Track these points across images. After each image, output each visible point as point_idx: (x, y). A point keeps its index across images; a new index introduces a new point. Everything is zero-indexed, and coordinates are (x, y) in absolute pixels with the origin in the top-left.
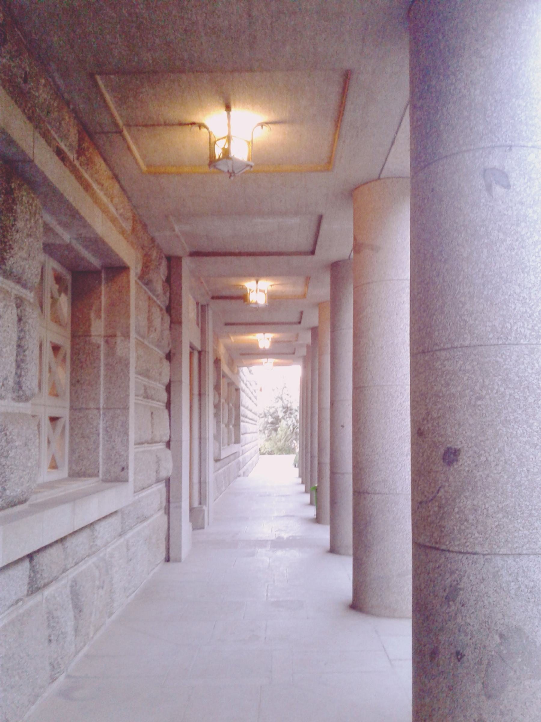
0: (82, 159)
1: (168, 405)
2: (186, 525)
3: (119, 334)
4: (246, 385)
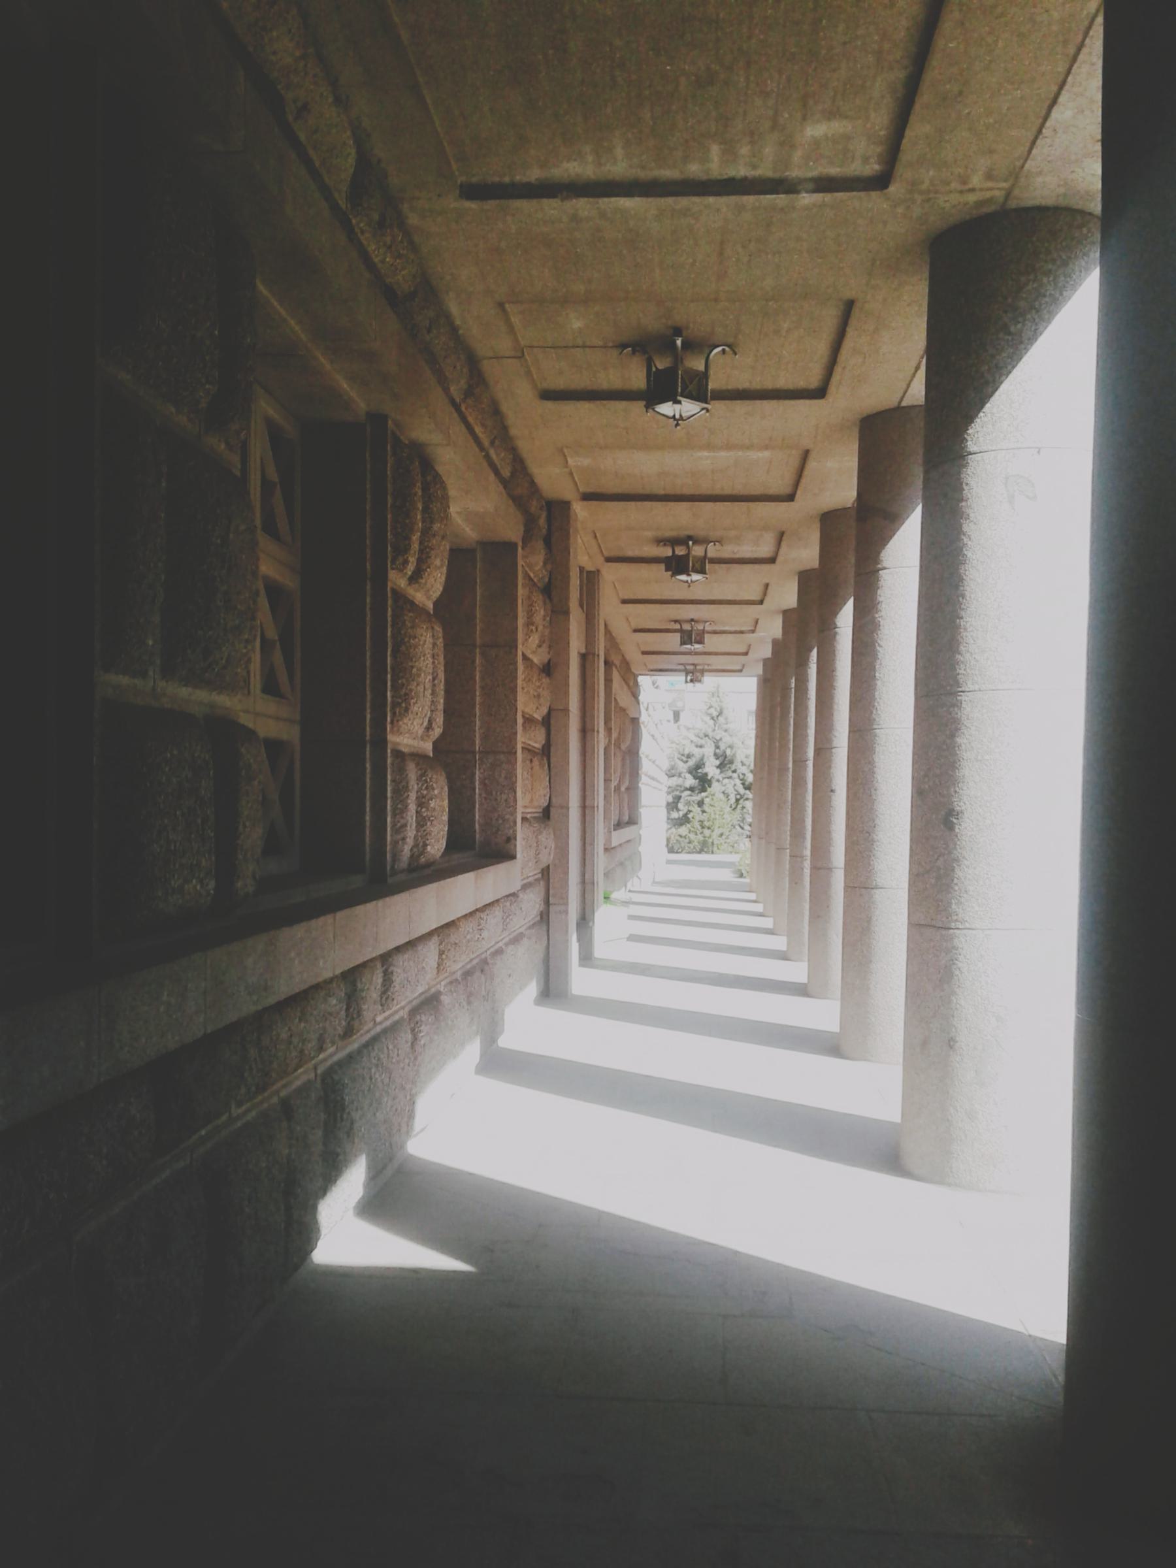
0: (470, 401)
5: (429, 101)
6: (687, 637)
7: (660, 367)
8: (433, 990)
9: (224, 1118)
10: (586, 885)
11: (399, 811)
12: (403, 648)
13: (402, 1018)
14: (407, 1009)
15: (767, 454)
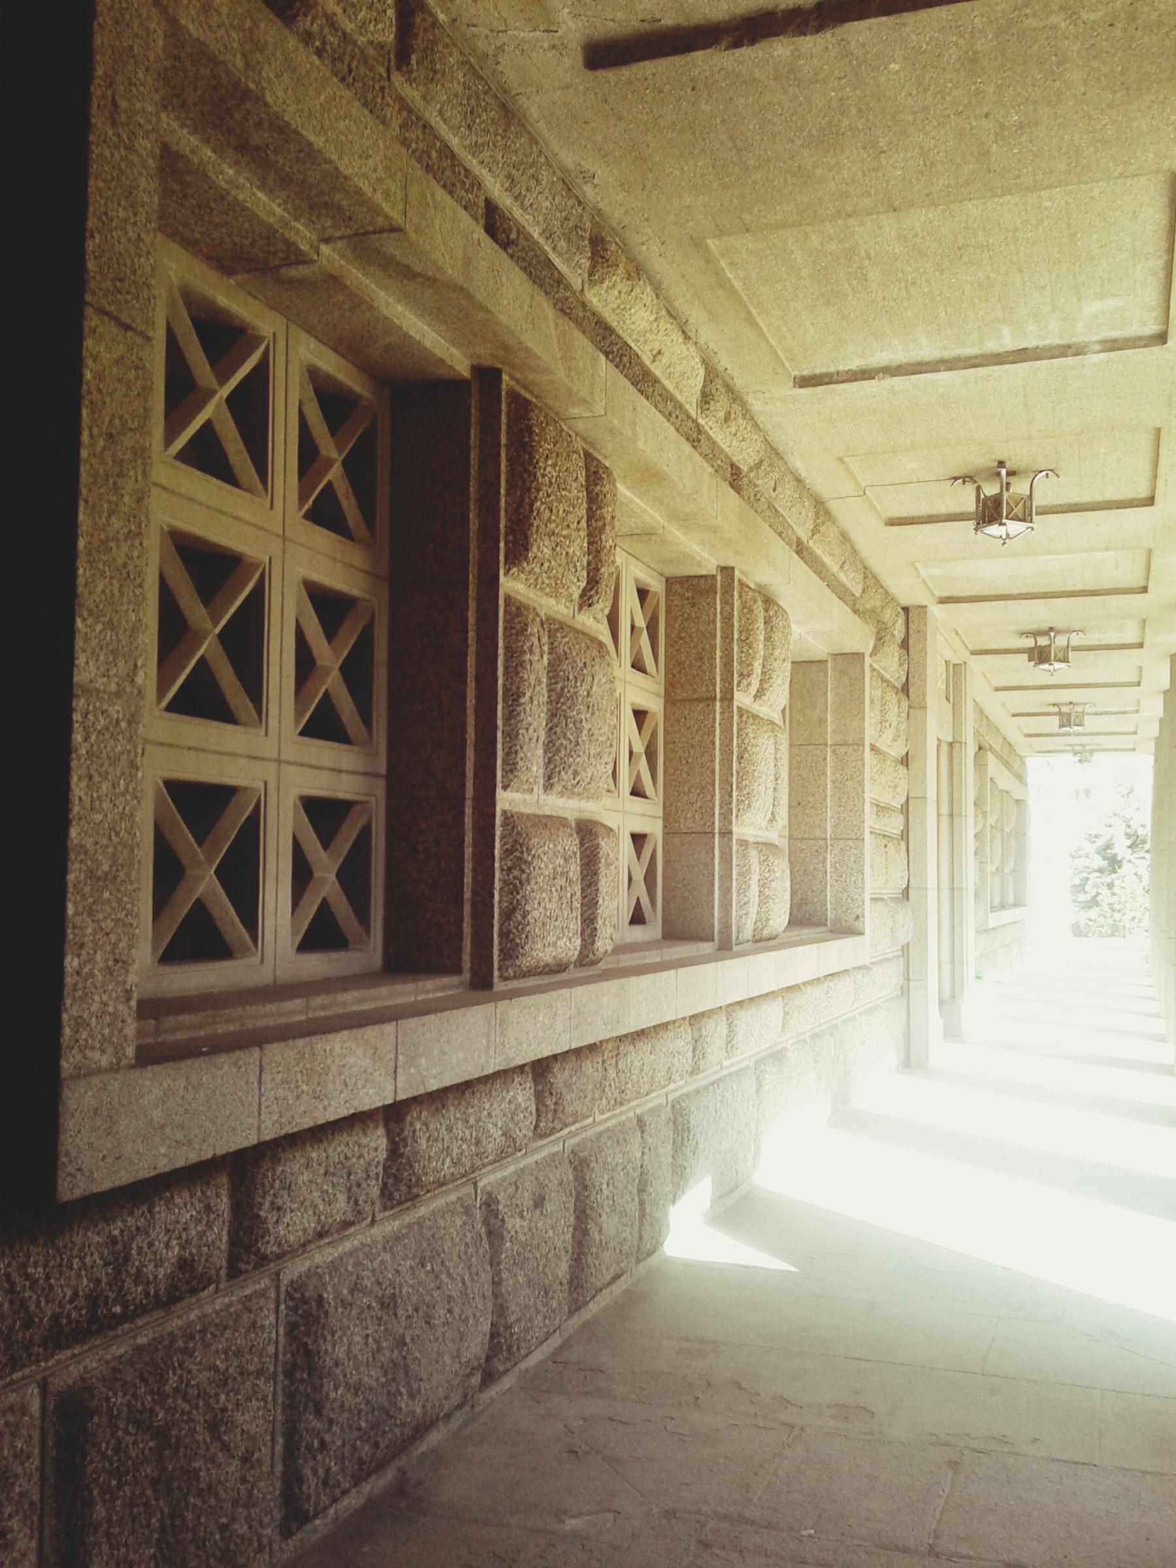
2: (935, 1022)
5: (762, 324)
6: (1066, 720)
7: (988, 494)
8: (780, 1047)
9: (590, 1120)
10: (955, 962)
11: (743, 891)
12: (746, 755)
13: (748, 1067)
14: (753, 1060)
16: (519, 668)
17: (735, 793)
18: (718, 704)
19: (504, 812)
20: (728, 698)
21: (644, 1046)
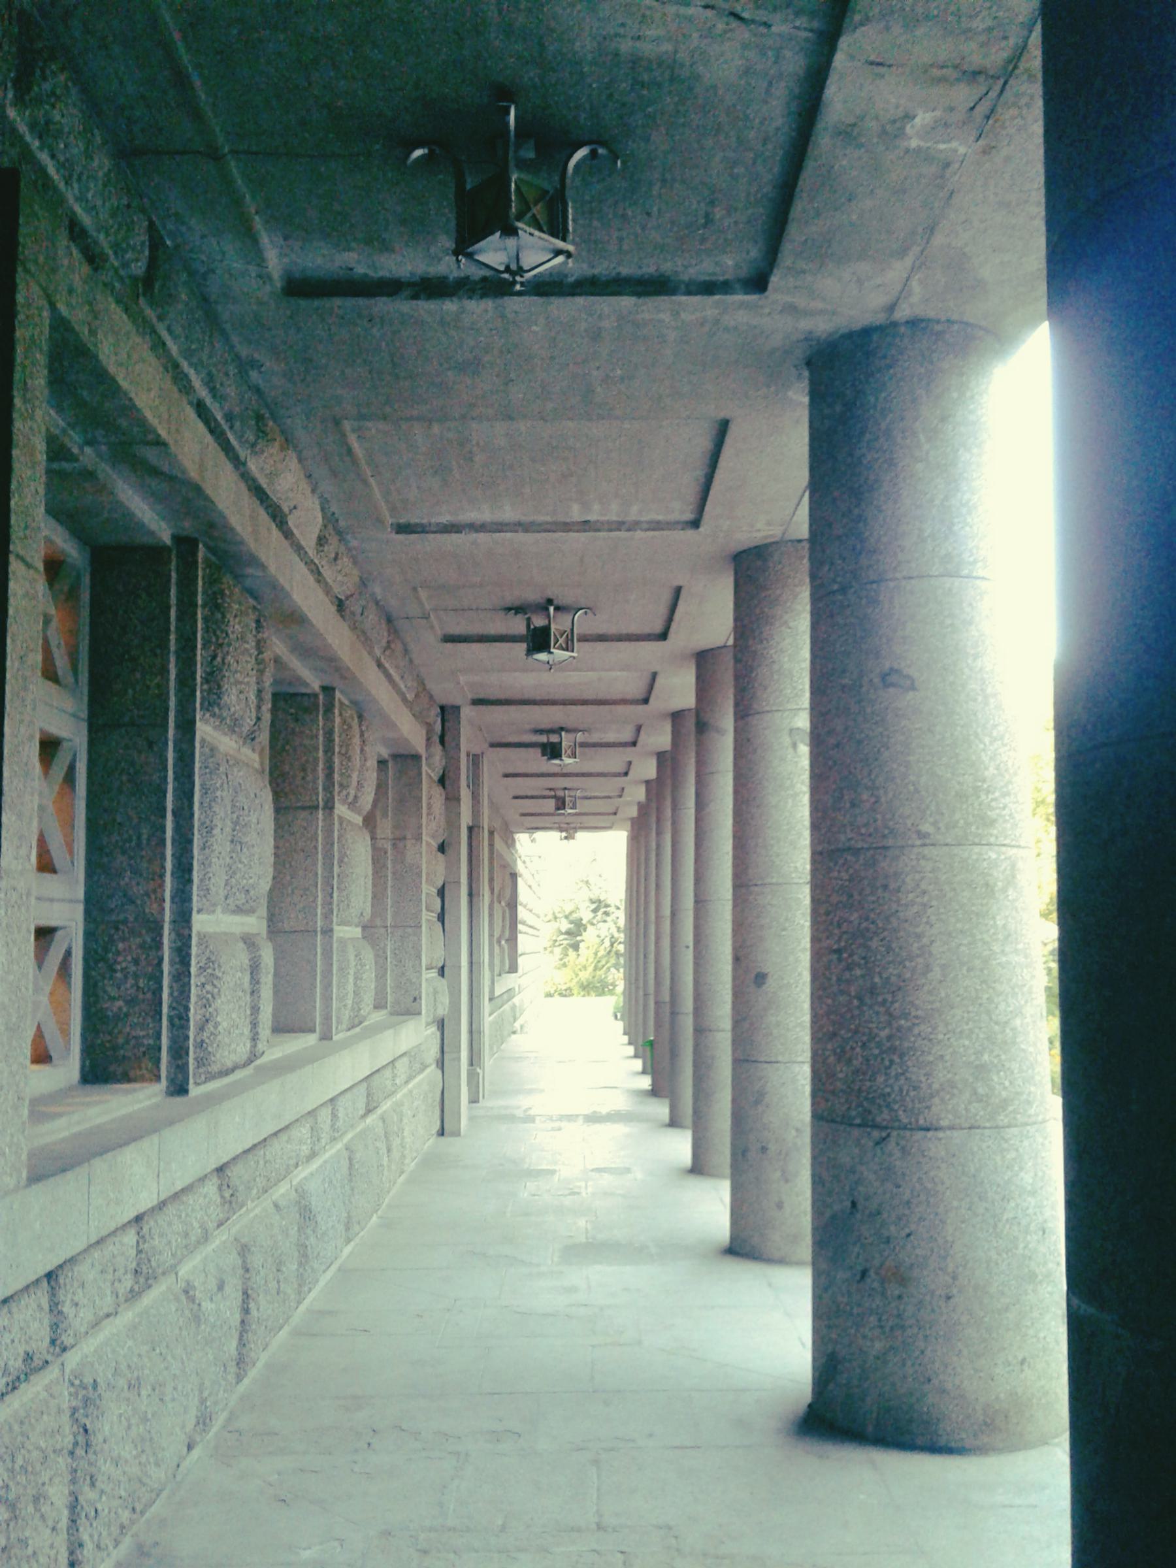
0: (387, 653)
1: (441, 918)
3: (409, 836)
4: (524, 862)
6: (561, 804)
9: (244, 1209)
12: (346, 860)
15: (625, 673)
16: (213, 804)
17: (335, 895)
18: (321, 812)
19: (199, 933)
20: (329, 807)
21: (284, 1137)
